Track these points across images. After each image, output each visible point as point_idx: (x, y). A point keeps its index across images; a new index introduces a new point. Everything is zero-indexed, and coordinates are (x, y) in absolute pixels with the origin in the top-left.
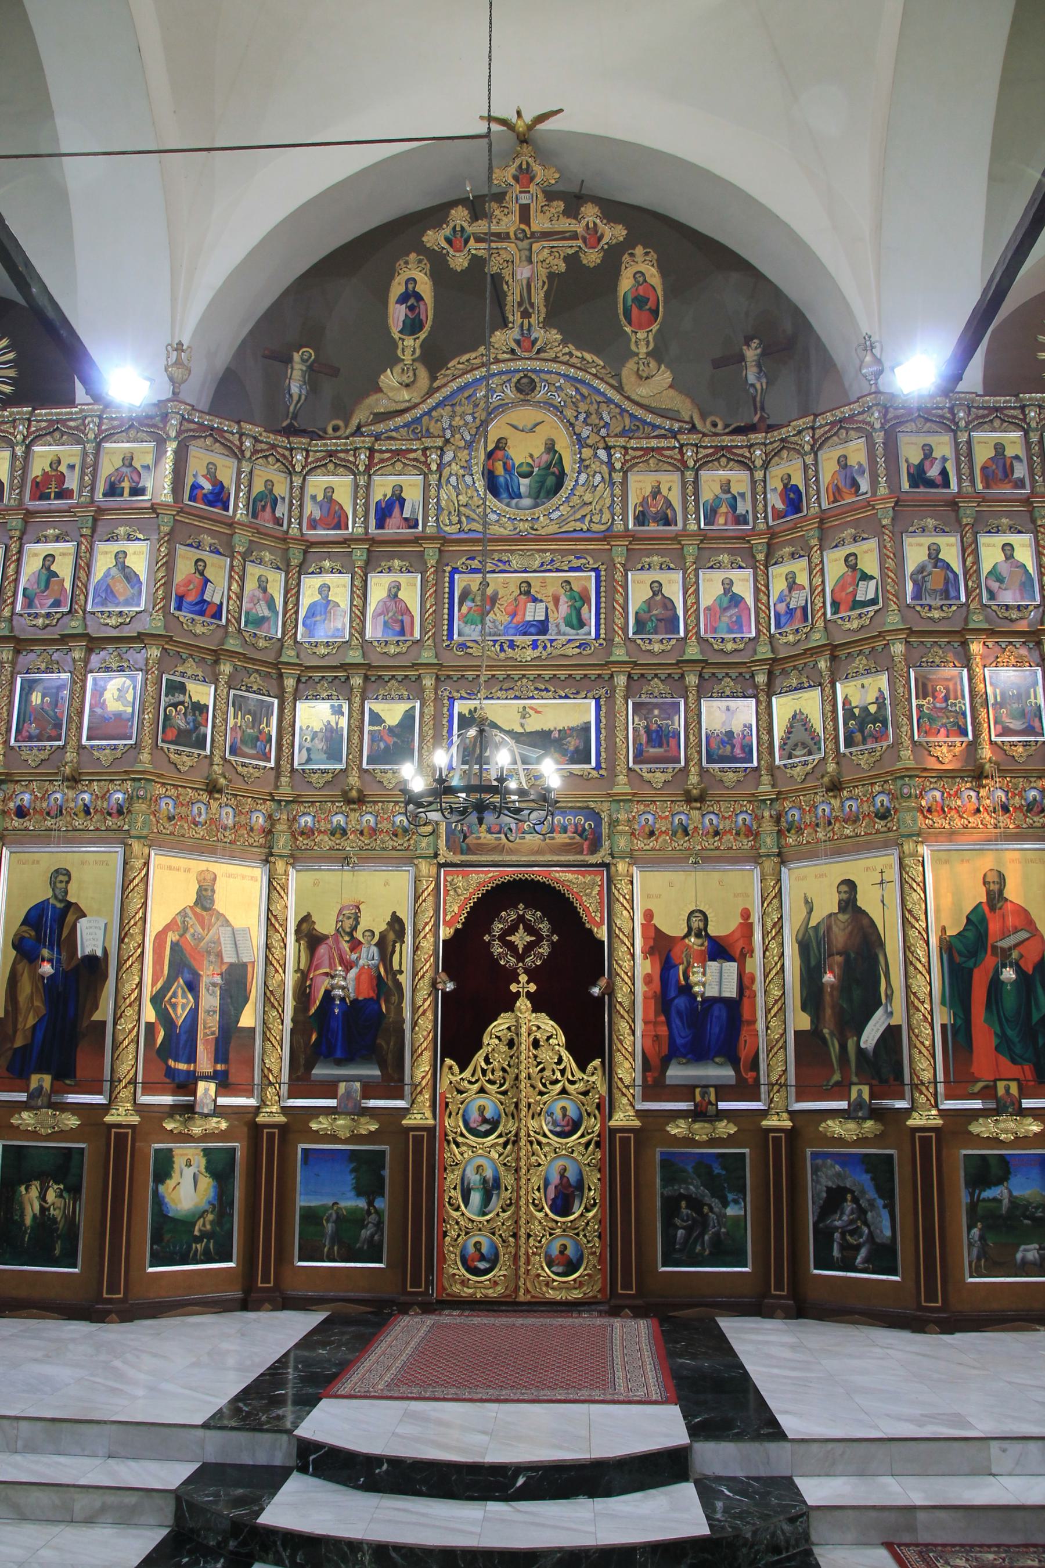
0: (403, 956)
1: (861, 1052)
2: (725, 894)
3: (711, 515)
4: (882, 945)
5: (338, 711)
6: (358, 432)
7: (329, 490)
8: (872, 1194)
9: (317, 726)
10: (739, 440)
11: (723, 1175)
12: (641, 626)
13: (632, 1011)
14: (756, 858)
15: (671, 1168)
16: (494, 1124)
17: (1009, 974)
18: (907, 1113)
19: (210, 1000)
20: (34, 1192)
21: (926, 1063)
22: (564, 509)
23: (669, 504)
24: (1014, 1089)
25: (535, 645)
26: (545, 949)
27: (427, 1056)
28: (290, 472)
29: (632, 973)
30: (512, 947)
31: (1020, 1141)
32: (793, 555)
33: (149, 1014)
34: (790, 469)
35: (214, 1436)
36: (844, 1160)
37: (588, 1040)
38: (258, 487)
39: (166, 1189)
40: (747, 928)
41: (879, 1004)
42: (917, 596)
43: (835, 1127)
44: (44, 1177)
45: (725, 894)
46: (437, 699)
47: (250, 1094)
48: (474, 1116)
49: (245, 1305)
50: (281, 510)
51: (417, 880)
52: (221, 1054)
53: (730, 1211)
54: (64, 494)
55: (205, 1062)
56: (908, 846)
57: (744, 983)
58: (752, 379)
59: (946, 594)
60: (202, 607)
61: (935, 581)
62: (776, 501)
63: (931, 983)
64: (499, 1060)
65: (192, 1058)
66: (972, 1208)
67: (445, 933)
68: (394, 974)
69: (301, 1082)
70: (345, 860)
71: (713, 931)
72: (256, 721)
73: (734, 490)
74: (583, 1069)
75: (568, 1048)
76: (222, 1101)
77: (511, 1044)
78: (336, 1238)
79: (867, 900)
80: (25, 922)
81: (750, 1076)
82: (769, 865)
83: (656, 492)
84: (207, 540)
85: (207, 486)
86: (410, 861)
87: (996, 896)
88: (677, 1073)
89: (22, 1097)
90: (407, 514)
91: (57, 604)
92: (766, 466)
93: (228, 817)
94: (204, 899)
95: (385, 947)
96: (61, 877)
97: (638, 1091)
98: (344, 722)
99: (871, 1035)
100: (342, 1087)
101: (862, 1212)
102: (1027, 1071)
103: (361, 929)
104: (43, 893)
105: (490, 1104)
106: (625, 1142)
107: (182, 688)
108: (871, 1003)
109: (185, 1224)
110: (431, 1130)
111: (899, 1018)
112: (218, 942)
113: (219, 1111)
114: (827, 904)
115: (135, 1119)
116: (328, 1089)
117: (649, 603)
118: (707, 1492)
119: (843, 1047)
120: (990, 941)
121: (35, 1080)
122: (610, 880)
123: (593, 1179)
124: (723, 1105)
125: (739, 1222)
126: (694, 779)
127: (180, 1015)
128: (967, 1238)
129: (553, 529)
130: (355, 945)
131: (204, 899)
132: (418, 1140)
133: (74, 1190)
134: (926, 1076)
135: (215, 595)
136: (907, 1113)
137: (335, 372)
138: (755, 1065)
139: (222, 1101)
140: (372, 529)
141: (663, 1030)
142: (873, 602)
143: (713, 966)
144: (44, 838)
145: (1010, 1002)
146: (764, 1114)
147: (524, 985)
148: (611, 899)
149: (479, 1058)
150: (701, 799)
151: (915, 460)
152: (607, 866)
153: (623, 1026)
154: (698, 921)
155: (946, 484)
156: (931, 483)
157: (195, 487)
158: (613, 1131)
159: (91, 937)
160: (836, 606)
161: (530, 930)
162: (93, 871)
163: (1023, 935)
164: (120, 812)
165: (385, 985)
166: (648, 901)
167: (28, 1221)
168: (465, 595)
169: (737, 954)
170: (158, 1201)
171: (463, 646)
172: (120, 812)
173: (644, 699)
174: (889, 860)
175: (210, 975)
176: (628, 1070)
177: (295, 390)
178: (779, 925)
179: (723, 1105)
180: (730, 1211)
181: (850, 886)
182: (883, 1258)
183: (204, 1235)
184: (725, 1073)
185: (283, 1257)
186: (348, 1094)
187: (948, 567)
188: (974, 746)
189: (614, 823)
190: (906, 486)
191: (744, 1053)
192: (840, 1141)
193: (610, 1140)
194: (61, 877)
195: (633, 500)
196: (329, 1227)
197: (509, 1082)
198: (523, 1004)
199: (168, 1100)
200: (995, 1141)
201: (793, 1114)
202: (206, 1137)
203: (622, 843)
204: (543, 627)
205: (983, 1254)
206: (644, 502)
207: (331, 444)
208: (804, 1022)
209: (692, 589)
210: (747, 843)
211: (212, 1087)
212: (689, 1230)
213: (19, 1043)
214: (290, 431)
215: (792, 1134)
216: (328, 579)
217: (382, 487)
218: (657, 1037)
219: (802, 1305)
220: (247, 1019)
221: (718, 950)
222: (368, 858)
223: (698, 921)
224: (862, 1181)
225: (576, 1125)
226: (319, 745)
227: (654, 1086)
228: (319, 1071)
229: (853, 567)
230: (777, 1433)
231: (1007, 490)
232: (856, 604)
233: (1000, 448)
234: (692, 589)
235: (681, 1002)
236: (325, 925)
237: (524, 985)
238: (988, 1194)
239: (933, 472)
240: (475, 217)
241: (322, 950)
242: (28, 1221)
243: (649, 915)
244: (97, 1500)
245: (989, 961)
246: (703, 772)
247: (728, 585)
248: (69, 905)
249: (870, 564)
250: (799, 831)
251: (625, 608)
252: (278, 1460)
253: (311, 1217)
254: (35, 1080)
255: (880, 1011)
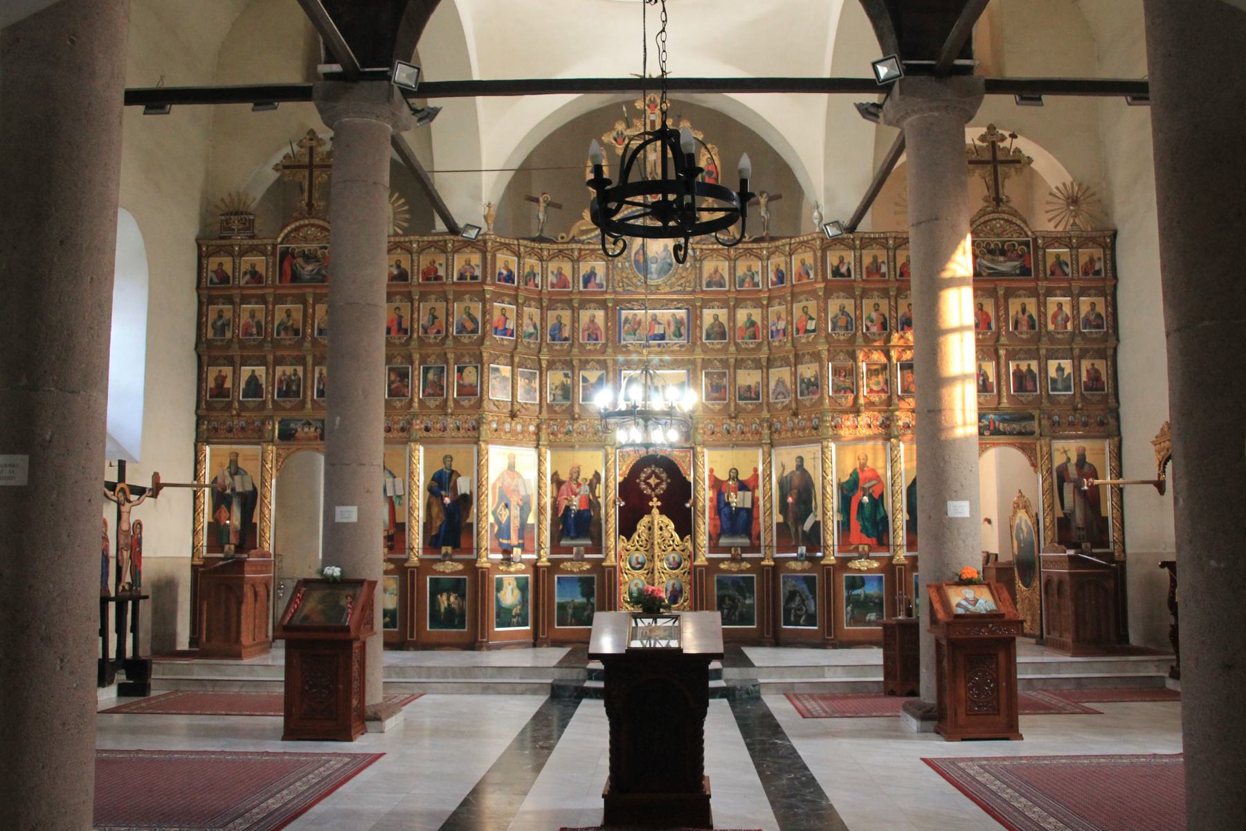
0: (600, 490)
1: (804, 532)
2: (749, 461)
3: (742, 283)
4: (813, 485)
5: (566, 376)
6: (573, 240)
7: (560, 269)
8: (807, 593)
9: (558, 383)
10: (755, 246)
11: (744, 586)
12: (708, 337)
13: (704, 513)
14: (759, 445)
15: (720, 583)
16: (643, 564)
17: (866, 499)
18: (822, 558)
19: (515, 512)
20: (444, 597)
21: (831, 537)
22: (673, 279)
23: (722, 277)
24: (866, 548)
25: (659, 345)
26: (664, 486)
27: (613, 535)
28: (541, 260)
29: (704, 496)
30: (649, 485)
31: (869, 570)
32: (780, 304)
33: (491, 519)
34: (779, 260)
35: (557, 671)
36: (797, 578)
37: (685, 526)
38: (527, 270)
39: (500, 595)
40: (756, 476)
41: (811, 511)
42: (833, 329)
43: (793, 565)
44: (449, 591)
45: (749, 461)
46: (614, 370)
47: (533, 552)
48: (634, 561)
49: (535, 645)
50: (538, 280)
51: (606, 456)
52: (521, 536)
53: (748, 602)
54: (438, 278)
55: (514, 540)
56: (825, 443)
57: (754, 501)
58: (763, 213)
59: (846, 328)
60: (506, 332)
61: (842, 322)
62: (772, 276)
63: (833, 503)
64: (644, 536)
65: (509, 538)
66: (848, 598)
67: (620, 479)
68: (596, 498)
69: (555, 548)
70: (572, 447)
71: (741, 477)
72: (530, 382)
73: (754, 270)
74: (682, 539)
75: (676, 530)
76: (525, 556)
77: (650, 529)
78: (574, 616)
79: (808, 466)
80: (433, 479)
81: (756, 543)
82: (766, 449)
83: (716, 271)
84: (507, 299)
85: (505, 272)
86: (603, 447)
87: (863, 466)
88: (723, 541)
89: (438, 557)
90: (598, 281)
91: (439, 332)
92: (768, 259)
93: (519, 428)
94: (512, 467)
95: (593, 485)
96: (448, 459)
97: (706, 549)
98: (569, 381)
99: (808, 525)
100: (575, 550)
101: (803, 601)
102: (874, 540)
103: (581, 476)
104: (439, 466)
105: (641, 556)
106: (701, 572)
107: (497, 370)
108: (809, 511)
109: (508, 611)
110: (615, 567)
111: (819, 518)
112: (517, 485)
113: (522, 561)
114: (791, 467)
115: (488, 565)
116: (569, 550)
117: (712, 326)
118: (726, 681)
119: (797, 530)
120: (861, 484)
121: (444, 550)
122: (695, 456)
123: (687, 588)
124: (744, 555)
125: (752, 605)
126: (732, 408)
127: (504, 519)
128: (845, 611)
129: (667, 289)
130: (579, 485)
131: (512, 467)
132: (610, 573)
133: (463, 596)
134: (830, 542)
135: (511, 325)
136: (822, 558)
137: (560, 207)
138: (758, 538)
139: (525, 556)
140: (581, 288)
141: (718, 522)
142: (814, 331)
143: (740, 493)
144: (440, 441)
145: (867, 511)
146: (763, 559)
147: (655, 503)
148: (695, 465)
149: (635, 536)
150: (735, 417)
151: (835, 264)
152: (693, 448)
153: (700, 521)
154: (734, 474)
155: (849, 275)
156: (842, 275)
157: (500, 274)
158: (695, 567)
159: (463, 485)
160: (798, 330)
161: (657, 477)
162: (461, 456)
163: (874, 482)
164: (474, 429)
165: (593, 504)
166: (710, 466)
167: (442, 610)
168: (626, 320)
169: (751, 487)
170: (498, 600)
171: (626, 346)
172: (474, 429)
173: (710, 370)
174: (817, 447)
175: (514, 501)
176: (703, 540)
177: (541, 217)
178: (770, 476)
179: (744, 555)
180: (748, 602)
181: (801, 459)
182: (811, 620)
183: (517, 615)
184: (745, 541)
185: (551, 624)
186: (578, 552)
187: (848, 315)
188: (856, 398)
189: (696, 429)
190: (829, 276)
191: (754, 533)
192: (794, 571)
193: (694, 571)
194: (448, 459)
195: (705, 275)
196: (570, 611)
197: (649, 546)
198: (655, 511)
199: (500, 556)
200: (859, 571)
201: (775, 560)
202: (516, 572)
203: (699, 438)
204: (662, 337)
205: (852, 617)
206: (710, 276)
207: (561, 247)
208: (781, 519)
209: (732, 318)
210: (757, 438)
211: (519, 550)
212: (729, 610)
213: (434, 533)
214: (541, 240)
215: (774, 568)
216: (559, 312)
217: (584, 268)
218: (715, 526)
219: (777, 641)
220: (531, 519)
221: (743, 486)
222: (584, 446)
223: (734, 474)
224: (803, 587)
225: (679, 565)
226: (559, 392)
227: (714, 548)
228: (564, 542)
229: (806, 313)
230: (753, 666)
231: (877, 278)
232: (807, 331)
233: (875, 258)
234: (732, 318)
235: (726, 510)
236: (564, 476)
237: (655, 503)
238: (855, 592)
239: (843, 270)
240: (628, 126)
241: (563, 487)
242: (442, 610)
243: (711, 471)
244: (524, 687)
245: (860, 493)
246: (736, 404)
247: (749, 316)
248: (453, 472)
249: (813, 312)
250: (780, 433)
251: (701, 328)
252: (581, 677)
253: (562, 607)
254: (444, 550)
255: (811, 516)
